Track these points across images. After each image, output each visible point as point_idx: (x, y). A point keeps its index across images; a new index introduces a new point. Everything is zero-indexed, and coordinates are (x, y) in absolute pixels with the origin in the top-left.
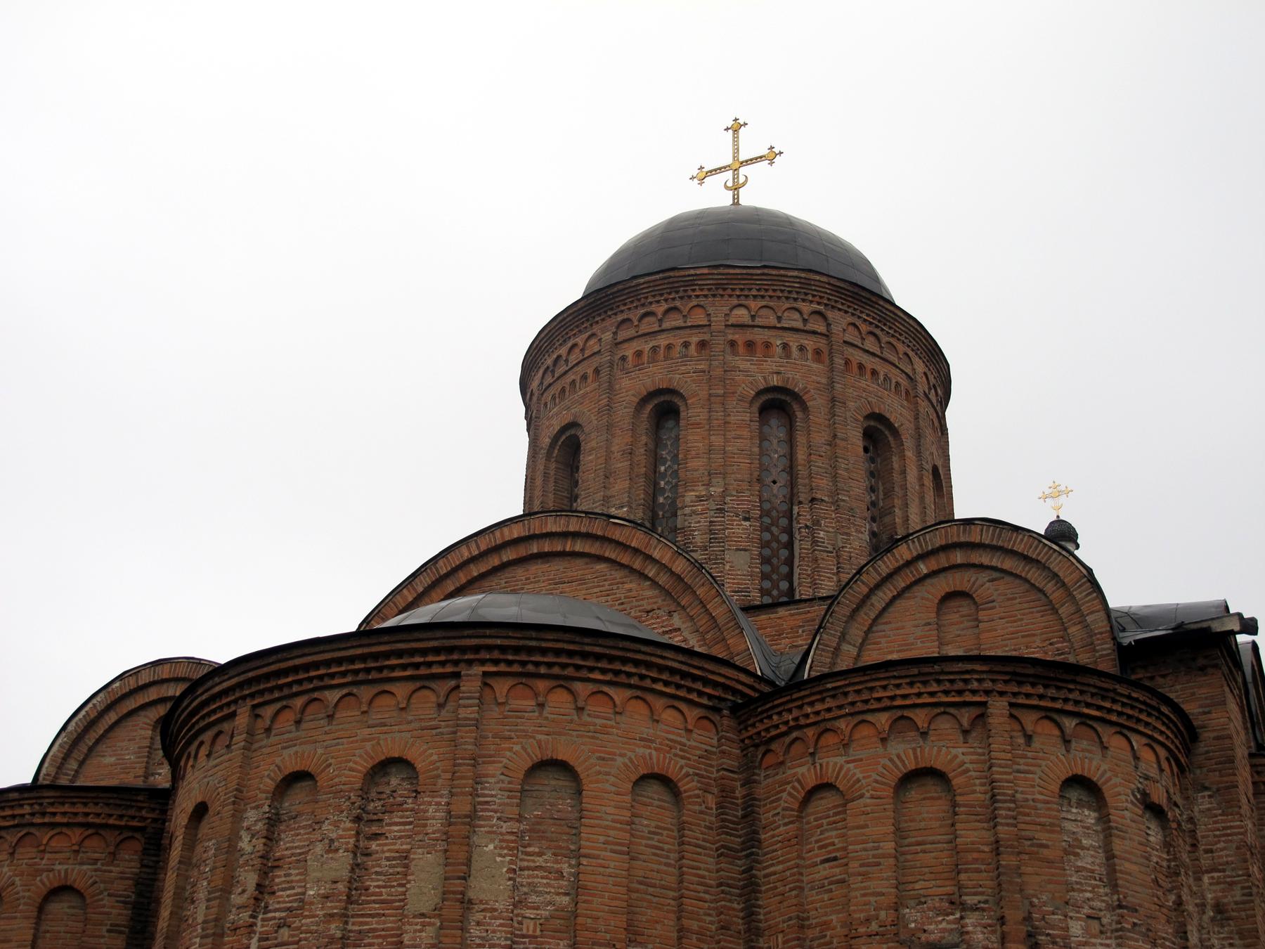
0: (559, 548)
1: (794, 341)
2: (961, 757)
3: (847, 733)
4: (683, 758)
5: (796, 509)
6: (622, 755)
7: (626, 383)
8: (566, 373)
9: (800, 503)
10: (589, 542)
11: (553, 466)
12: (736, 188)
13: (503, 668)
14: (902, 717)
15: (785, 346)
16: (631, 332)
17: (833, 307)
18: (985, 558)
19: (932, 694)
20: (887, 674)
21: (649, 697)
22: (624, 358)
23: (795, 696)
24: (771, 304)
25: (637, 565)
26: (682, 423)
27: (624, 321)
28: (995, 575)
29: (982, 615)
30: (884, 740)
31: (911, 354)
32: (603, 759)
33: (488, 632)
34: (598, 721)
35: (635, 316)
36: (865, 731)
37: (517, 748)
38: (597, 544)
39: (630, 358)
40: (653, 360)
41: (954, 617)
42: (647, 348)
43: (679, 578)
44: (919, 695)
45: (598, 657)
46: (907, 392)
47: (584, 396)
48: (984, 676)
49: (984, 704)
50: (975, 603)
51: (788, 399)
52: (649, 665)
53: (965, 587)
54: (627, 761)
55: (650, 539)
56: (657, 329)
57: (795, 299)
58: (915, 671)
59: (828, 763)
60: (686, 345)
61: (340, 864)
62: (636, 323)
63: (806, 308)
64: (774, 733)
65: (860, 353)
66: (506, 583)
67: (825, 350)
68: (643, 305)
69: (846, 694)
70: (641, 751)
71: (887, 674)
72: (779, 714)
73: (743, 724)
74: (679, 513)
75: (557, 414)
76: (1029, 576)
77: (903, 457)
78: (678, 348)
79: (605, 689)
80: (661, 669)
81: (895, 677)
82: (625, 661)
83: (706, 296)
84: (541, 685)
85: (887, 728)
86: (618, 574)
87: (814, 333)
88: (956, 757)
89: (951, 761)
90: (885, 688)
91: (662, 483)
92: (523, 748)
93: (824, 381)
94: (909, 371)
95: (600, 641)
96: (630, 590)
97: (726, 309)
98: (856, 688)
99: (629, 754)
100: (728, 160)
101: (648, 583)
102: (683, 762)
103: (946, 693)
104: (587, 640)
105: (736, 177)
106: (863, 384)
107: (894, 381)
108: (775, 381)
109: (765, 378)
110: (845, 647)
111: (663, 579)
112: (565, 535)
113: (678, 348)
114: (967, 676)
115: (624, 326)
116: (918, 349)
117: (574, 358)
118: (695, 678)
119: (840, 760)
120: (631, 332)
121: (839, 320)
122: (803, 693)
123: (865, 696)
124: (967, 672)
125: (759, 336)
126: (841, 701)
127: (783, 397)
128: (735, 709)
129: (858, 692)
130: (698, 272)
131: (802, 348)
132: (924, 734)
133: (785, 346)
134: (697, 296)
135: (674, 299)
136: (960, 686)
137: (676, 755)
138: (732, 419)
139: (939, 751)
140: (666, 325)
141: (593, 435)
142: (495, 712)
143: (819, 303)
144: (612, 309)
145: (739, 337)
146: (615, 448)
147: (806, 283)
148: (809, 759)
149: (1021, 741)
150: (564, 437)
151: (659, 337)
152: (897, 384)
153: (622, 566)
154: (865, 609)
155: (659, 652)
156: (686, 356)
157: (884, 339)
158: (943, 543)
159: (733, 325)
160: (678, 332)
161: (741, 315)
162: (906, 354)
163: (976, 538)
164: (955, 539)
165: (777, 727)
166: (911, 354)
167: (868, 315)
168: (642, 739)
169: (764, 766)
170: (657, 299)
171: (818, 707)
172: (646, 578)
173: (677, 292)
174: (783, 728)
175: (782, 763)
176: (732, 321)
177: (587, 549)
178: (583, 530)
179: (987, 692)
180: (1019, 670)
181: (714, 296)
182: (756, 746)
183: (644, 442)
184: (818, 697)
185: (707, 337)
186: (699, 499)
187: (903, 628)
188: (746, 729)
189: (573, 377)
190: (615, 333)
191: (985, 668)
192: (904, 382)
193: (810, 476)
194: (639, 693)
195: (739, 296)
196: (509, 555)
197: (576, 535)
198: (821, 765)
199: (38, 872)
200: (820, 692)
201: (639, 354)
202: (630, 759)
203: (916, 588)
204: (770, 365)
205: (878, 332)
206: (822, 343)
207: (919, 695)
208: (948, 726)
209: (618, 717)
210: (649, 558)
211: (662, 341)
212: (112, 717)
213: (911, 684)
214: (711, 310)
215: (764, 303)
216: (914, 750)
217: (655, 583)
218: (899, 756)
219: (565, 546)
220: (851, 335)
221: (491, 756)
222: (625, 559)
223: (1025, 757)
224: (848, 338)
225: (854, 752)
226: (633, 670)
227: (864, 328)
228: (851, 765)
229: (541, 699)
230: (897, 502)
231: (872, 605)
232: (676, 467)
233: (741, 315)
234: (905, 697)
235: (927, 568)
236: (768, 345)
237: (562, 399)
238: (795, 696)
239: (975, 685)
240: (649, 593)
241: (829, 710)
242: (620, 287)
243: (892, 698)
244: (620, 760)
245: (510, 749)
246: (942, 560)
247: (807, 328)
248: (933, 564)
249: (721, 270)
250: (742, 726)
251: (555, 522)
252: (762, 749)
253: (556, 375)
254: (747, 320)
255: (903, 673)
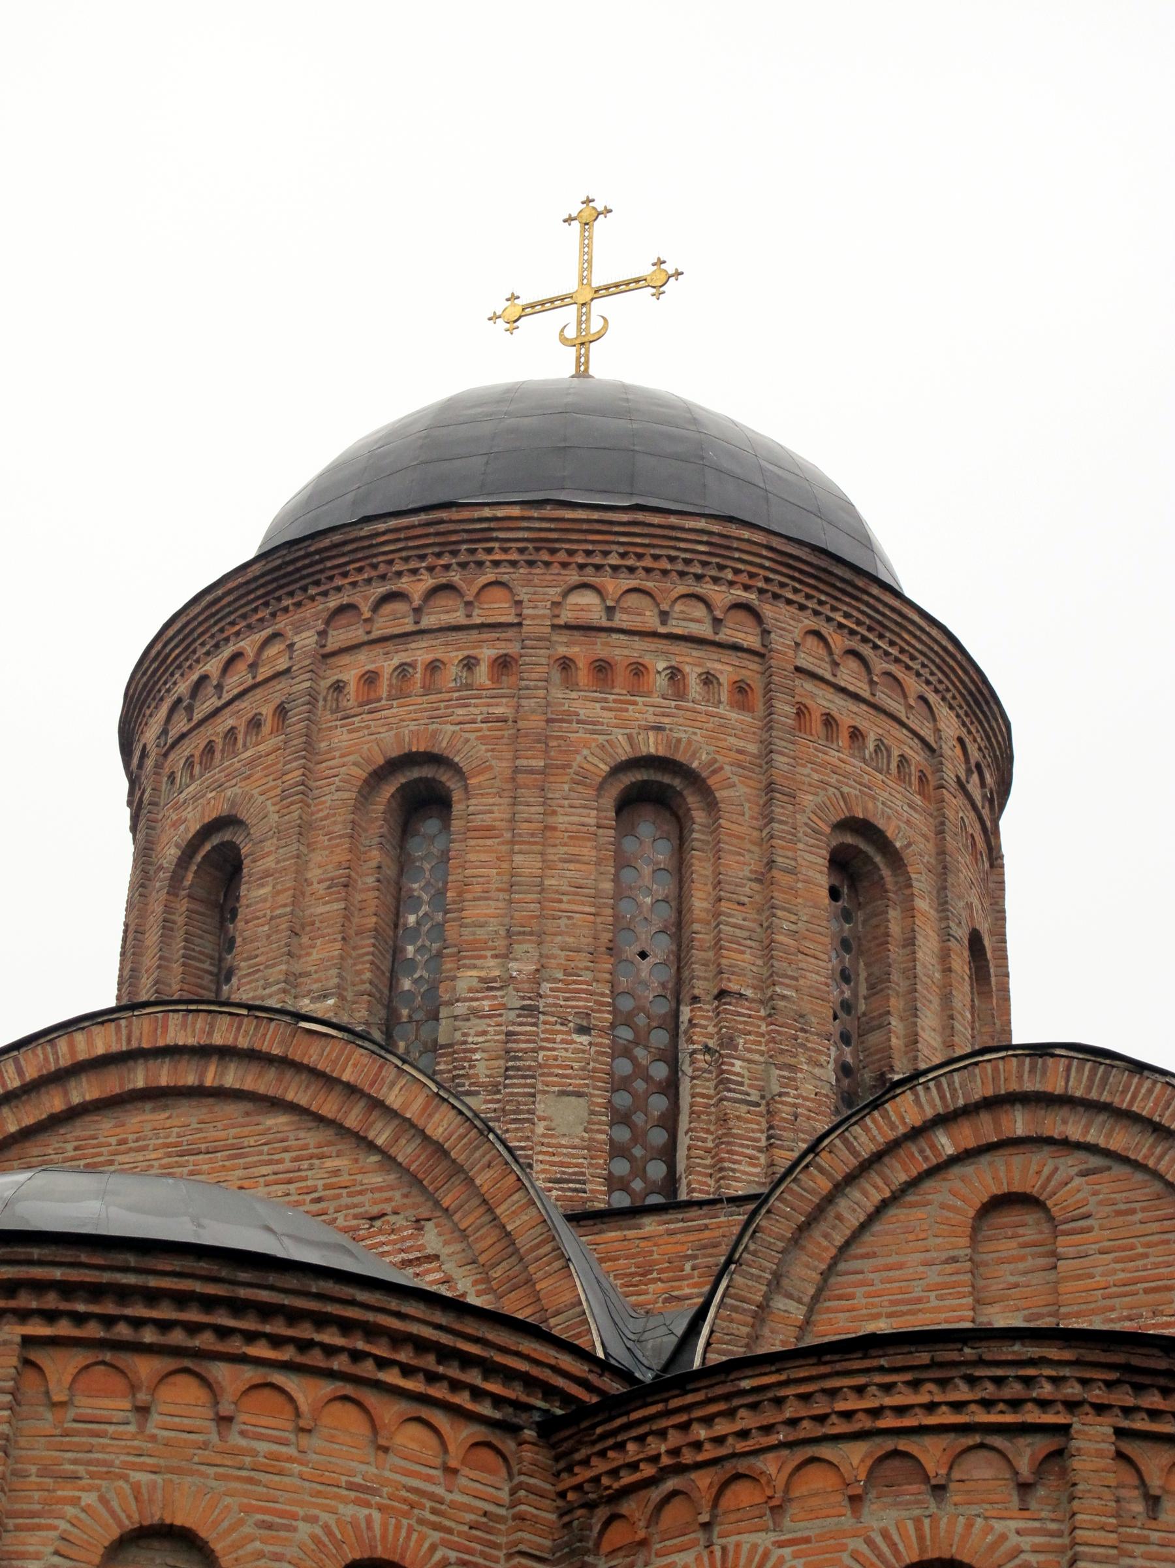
0: (191, 1080)
1: (693, 663)
2: (1014, 1540)
3: (780, 1481)
4: (436, 1527)
5: (686, 1012)
6: (309, 1519)
7: (341, 737)
8: (217, 711)
9: (695, 999)
10: (254, 1068)
11: (183, 906)
12: (583, 343)
13: (64, 1328)
14: (896, 1453)
15: (675, 673)
16: (357, 633)
17: (776, 596)
18: (1073, 1127)
19: (958, 1406)
20: (867, 1363)
21: (371, 1398)
22: (338, 687)
23: (674, 1403)
24: (649, 585)
25: (353, 1119)
26: (456, 825)
27: (342, 609)
28: (1095, 1161)
29: (1064, 1245)
30: (855, 1500)
31: (933, 698)
32: (270, 1526)
33: (36, 1252)
34: (263, 1447)
35: (365, 598)
36: (816, 1480)
37: (89, 1498)
38: (272, 1073)
39: (352, 688)
40: (400, 693)
41: (1008, 1247)
43: (440, 1150)
44: (931, 1407)
45: (266, 1311)
46: (922, 778)
47: (252, 763)
48: (1066, 1372)
49: (1064, 1429)
50: (1051, 1219)
51: (677, 783)
52: (371, 1332)
53: (1031, 1186)
54: (318, 1531)
55: (381, 1067)
56: (410, 628)
57: (699, 578)
58: (924, 1358)
59: (738, 1545)
60: (469, 664)
62: (367, 614)
63: (721, 596)
64: (627, 1479)
65: (830, 694)
66: (76, 1149)
67: (757, 683)
68: (383, 577)
69: (779, 1402)
70: (348, 1511)
71: (867, 1363)
72: (641, 1439)
73: (564, 1462)
74: (444, 1012)
75: (195, 798)
76: (1162, 1167)
77: (910, 911)
78: (453, 670)
79: (278, 1378)
80: (398, 1339)
81: (881, 1369)
82: (321, 1321)
83: (513, 564)
84: (145, 1368)
85: (862, 1476)
86: (312, 1138)
87: (736, 648)
88: (1003, 1537)
89: (993, 1547)
90: (860, 1390)
91: (410, 949)
92: (103, 1500)
93: (752, 748)
94: (926, 732)
95: (272, 1278)
96: (336, 1172)
97: (554, 593)
98: (803, 1389)
99: (325, 1517)
100: (569, 284)
101: (374, 1158)
102: (436, 1536)
103: (987, 1404)
104: (243, 1276)
105: (583, 321)
106: (833, 756)
107: (896, 753)
108: (651, 745)
109: (630, 738)
110: (780, 1303)
111: (407, 1151)
112: (203, 1052)
113: (453, 670)
114: (1030, 1372)
115: (342, 620)
116: (948, 690)
118: (467, 1361)
119: (764, 1540)
120: (353, 633)
122: (690, 1399)
123: (820, 1406)
124: (1032, 1362)
125: (620, 650)
126: (769, 1416)
127: (666, 779)
128: (548, 1428)
129: (805, 1398)
130: (500, 513)
131: (708, 679)
132: (939, 1490)
133: (675, 673)
134: (496, 564)
135: (447, 567)
136: (1015, 1390)
137: (421, 1521)
138: (561, 820)
139: (969, 1525)
140: (428, 621)
141: (268, 846)
142: (47, 1421)
143: (747, 588)
144: (317, 583)
145: (579, 651)
146: (314, 874)
147: (721, 547)
148: (700, 1535)
149: (1138, 1507)
150: (208, 847)
151: (413, 645)
153: (320, 1119)
154: (823, 1226)
155: (394, 1304)
156: (468, 687)
157: (879, 665)
158: (990, 1092)
159: (568, 627)
160: (452, 636)
161: (586, 607)
162: (922, 698)
163: (1055, 1084)
164: (1014, 1086)
165: (634, 1466)
166: (933, 698)
167: (847, 615)
168: (351, 1487)
169: (605, 1547)
170: (413, 565)
171: (722, 1427)
172: (371, 1147)
173: (454, 553)
174: (648, 1471)
175: (644, 1543)
176: (566, 616)
177: (249, 1084)
178: (243, 1043)
179: (1072, 1406)
180: (1136, 1361)
181: (531, 563)
182: (591, 1506)
183: (374, 864)
184: (722, 1406)
185: (513, 649)
186: (487, 985)
187: (900, 1266)
188: (569, 1469)
189: (231, 722)
190: (322, 634)
191: (1067, 1355)
192: (917, 756)
193: (718, 946)
194: (349, 1389)
195: (582, 567)
196: (83, 1091)
197: (226, 1053)
198: (724, 1549)
200: (727, 1397)
201: (370, 678)
202: (326, 1528)
203: (928, 1185)
204: (643, 711)
205: (866, 650)
206: (750, 670)
207: (931, 1407)
208: (988, 1473)
209: (304, 1440)
210: (377, 1105)
211: (420, 653)
213: (915, 1385)
214: (523, 594)
215: (633, 583)
216: (918, 1521)
217: (388, 1159)
218: (885, 1535)
219: (202, 1075)
220: (811, 657)
221: (33, 1515)
222: (329, 1106)
223: (1146, 1542)
224: (804, 661)
225: (795, 1524)
226: (339, 1341)
227: (839, 642)
228: (787, 1551)
229: (142, 1397)
230: (896, 1004)
231: (839, 1217)
232: (439, 917)
234: (901, 1410)
235: (955, 1143)
236: (638, 670)
237: (207, 767)
238: (674, 1403)
239: (1046, 1390)
240: (377, 1179)
241: (744, 1434)
242: (337, 538)
243: (876, 1413)
244: (304, 1528)
245: (75, 1501)
246: (986, 1129)
247: (721, 637)
248: (966, 1135)
249: (548, 512)
250: (562, 1465)
251: (184, 1025)
252: (602, 1513)
253: (197, 717)
254: (597, 616)
255: (900, 1361)
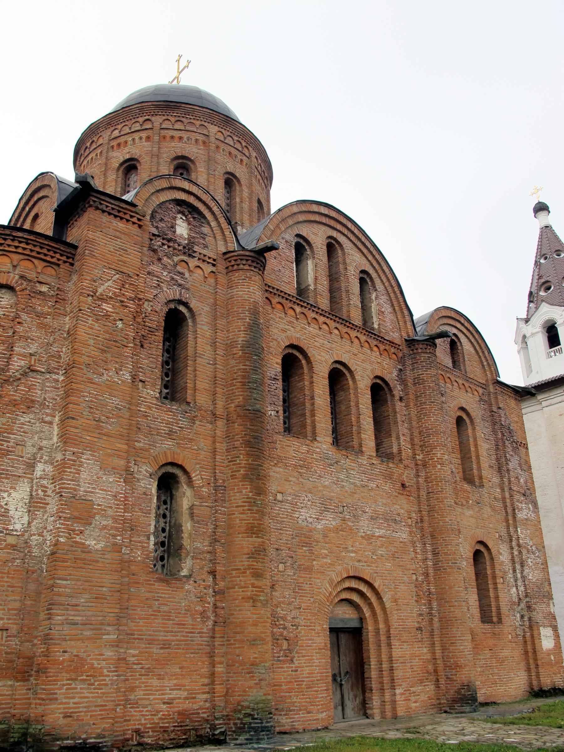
1: (136, 136)
17: (156, 115)
31: (206, 124)
46: (204, 143)
57: (138, 117)
60: (97, 155)
63: (141, 120)
65: (172, 131)
106: (173, 144)
108: (127, 157)
116: (214, 122)
121: (157, 120)
125: (122, 140)
138: (109, 179)
145: (114, 143)
152: (197, 140)
161: (116, 133)
166: (206, 124)
167: (177, 113)
176: (112, 137)
192: (201, 138)
204: (126, 150)
233: (116, 133)
247: (143, 128)
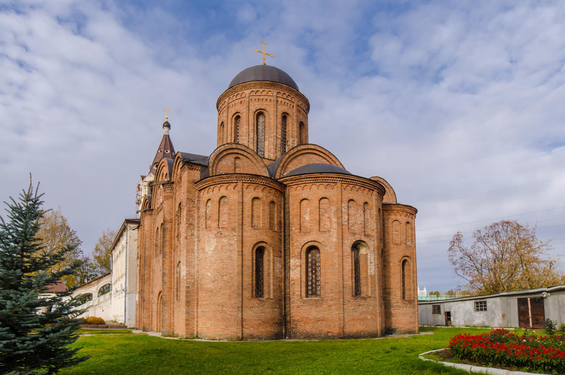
0: (319, 154)
36: (403, 214)
38: (326, 156)
42: (284, 101)
47: (267, 104)
61: (362, 219)
75: (258, 104)
117: (264, 93)
119: (400, 217)
178: (324, 152)
199: (268, 197)
211: (287, 101)
212: (225, 153)
253: (257, 94)
